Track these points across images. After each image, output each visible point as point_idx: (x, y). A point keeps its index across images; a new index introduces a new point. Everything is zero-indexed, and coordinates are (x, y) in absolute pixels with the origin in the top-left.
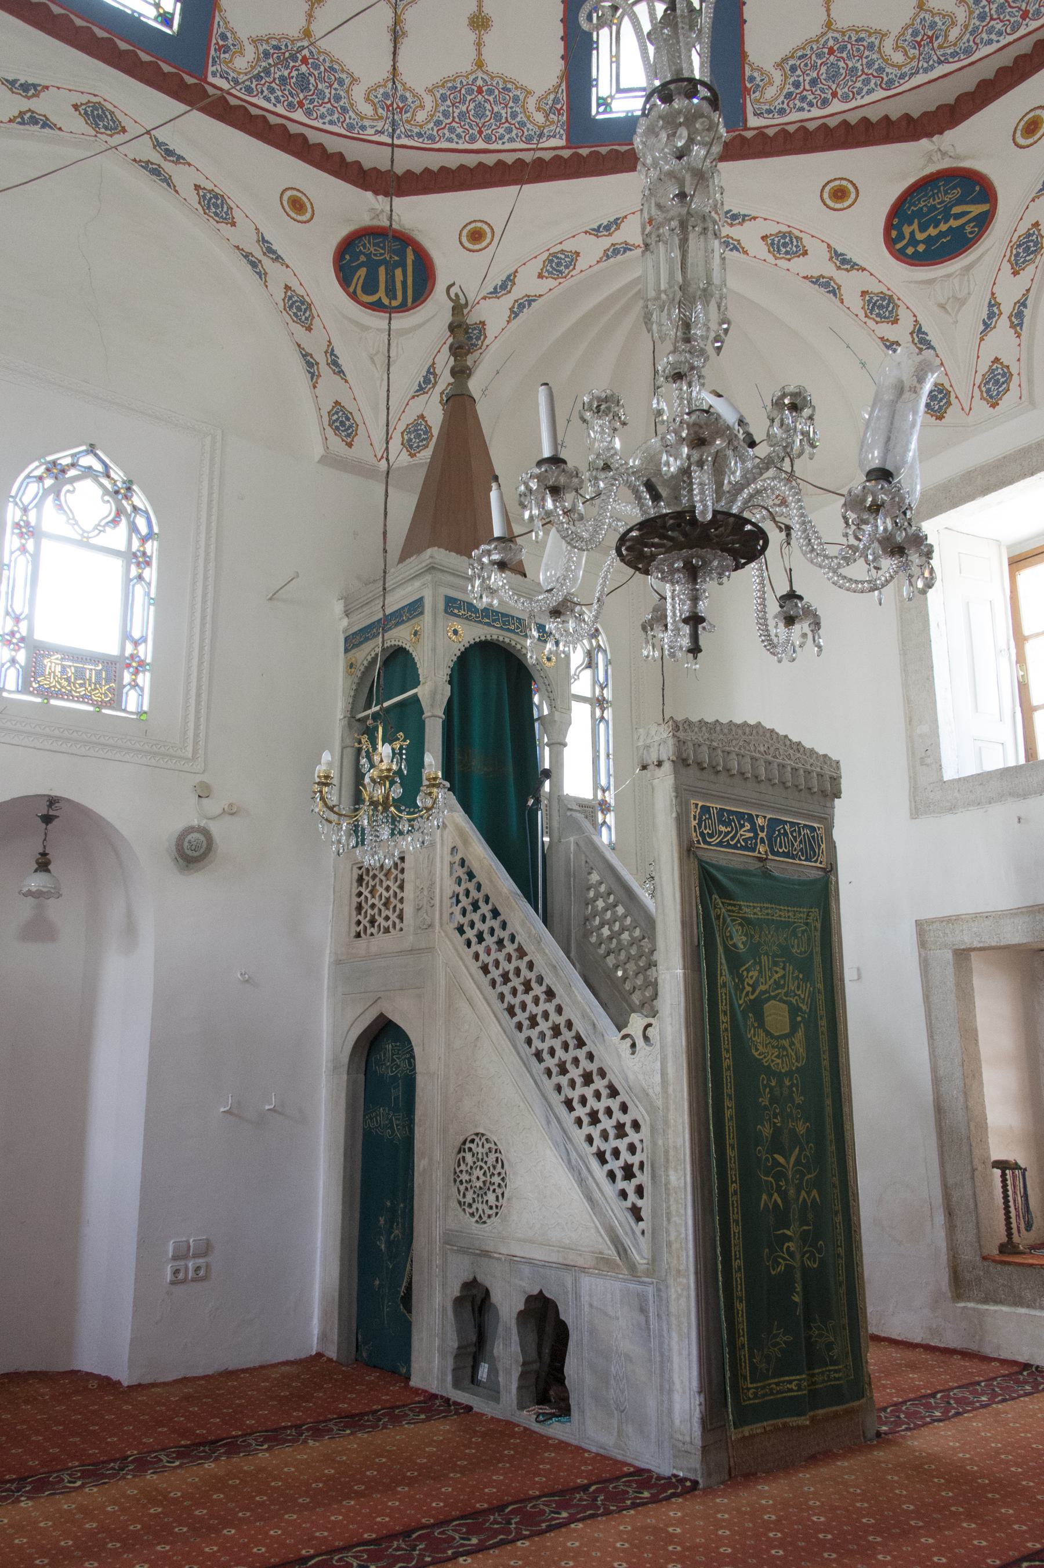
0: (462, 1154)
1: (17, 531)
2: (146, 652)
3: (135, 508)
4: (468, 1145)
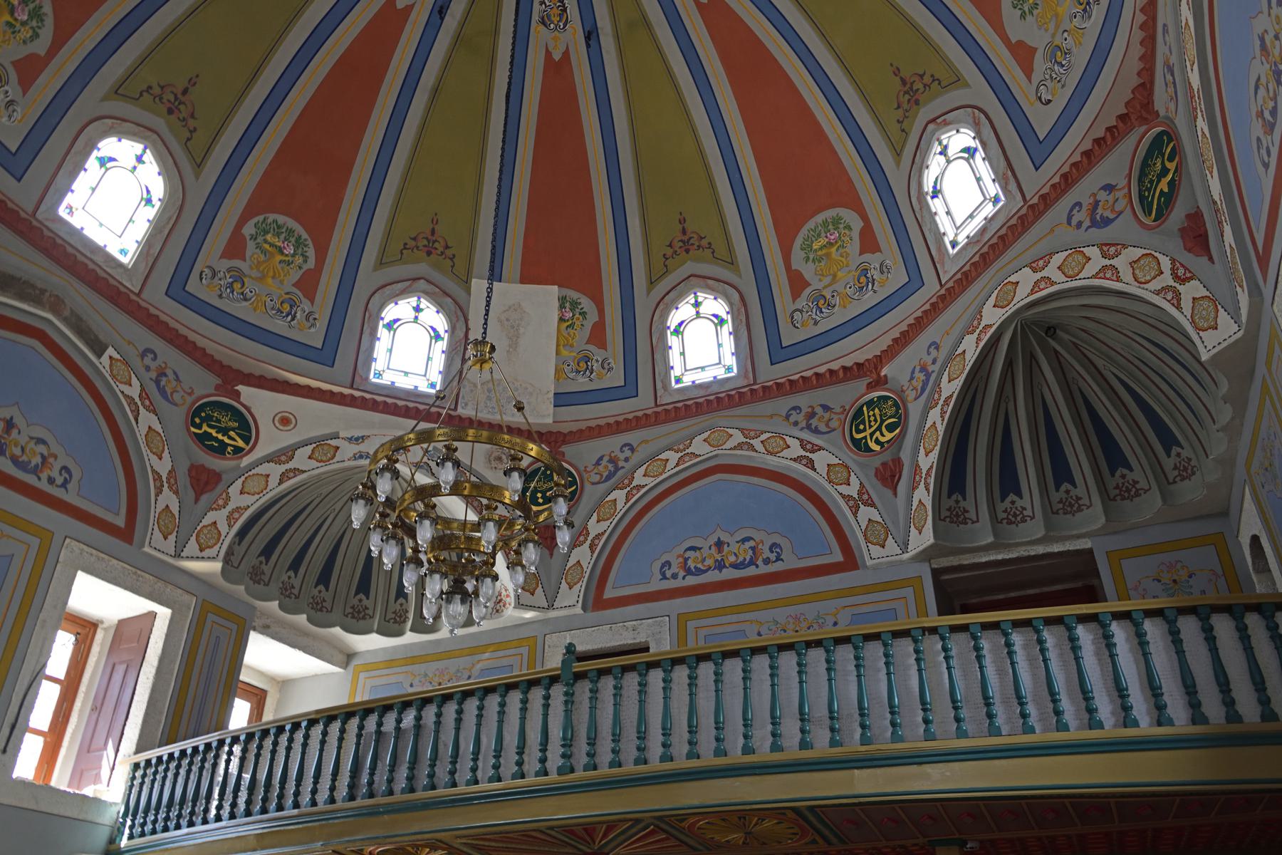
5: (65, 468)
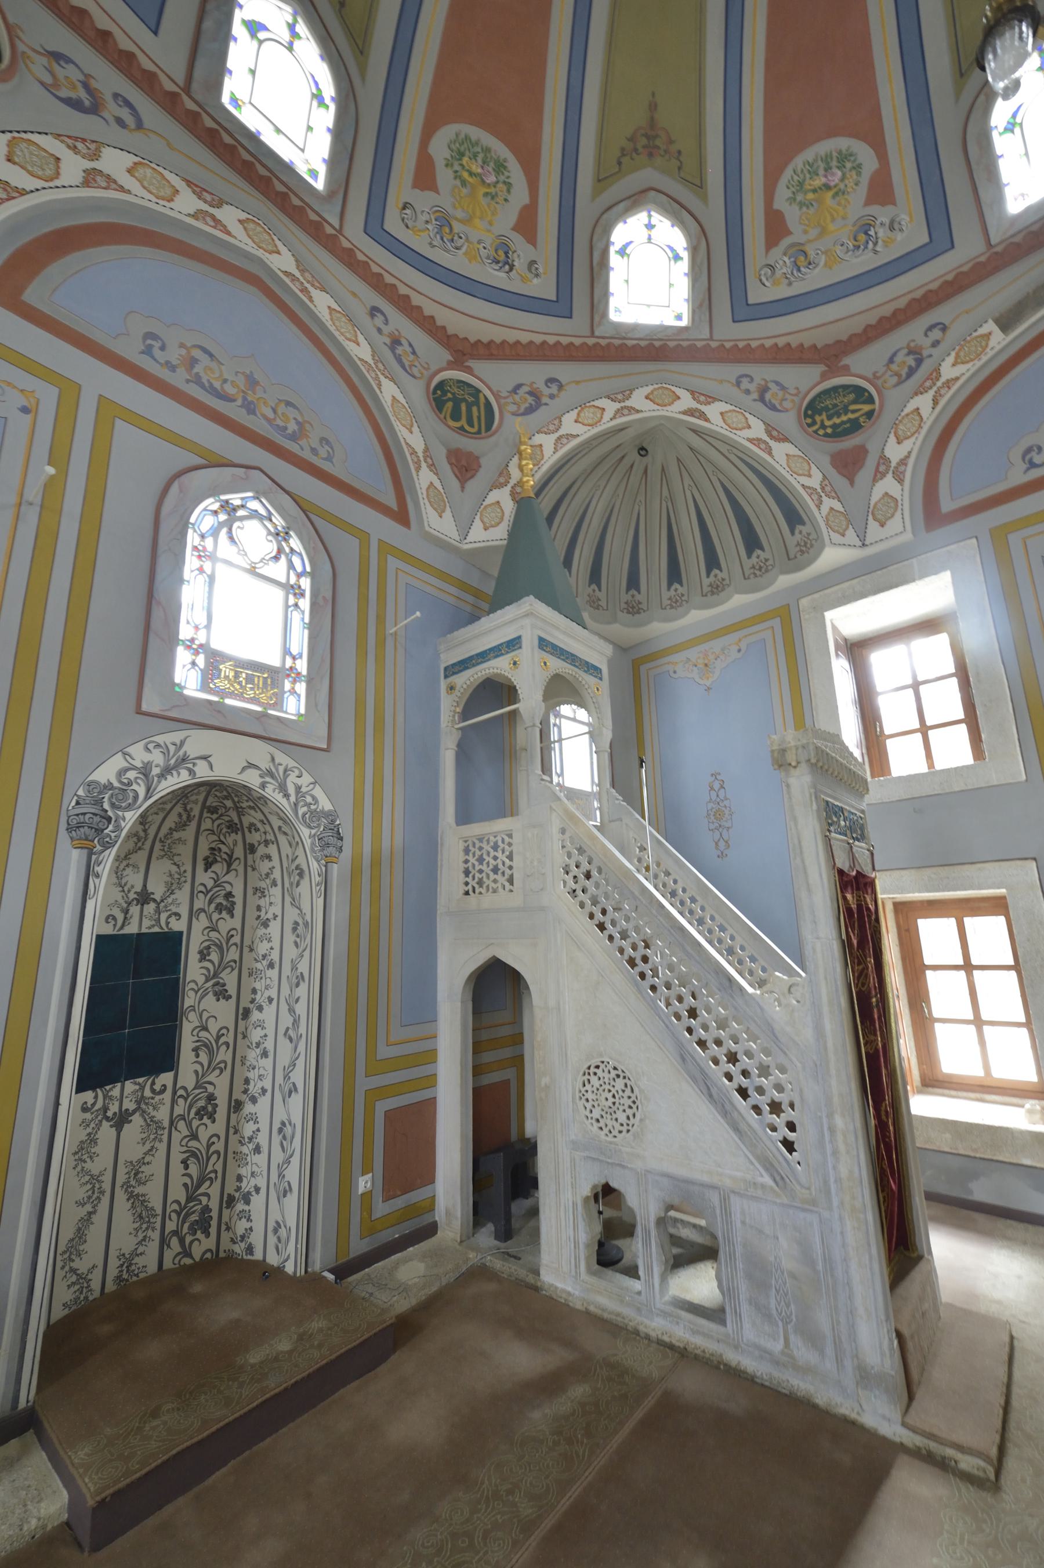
0: (587, 1077)
1: (196, 554)
2: (302, 666)
3: (292, 550)
4: (592, 1070)
5: (324, 440)
